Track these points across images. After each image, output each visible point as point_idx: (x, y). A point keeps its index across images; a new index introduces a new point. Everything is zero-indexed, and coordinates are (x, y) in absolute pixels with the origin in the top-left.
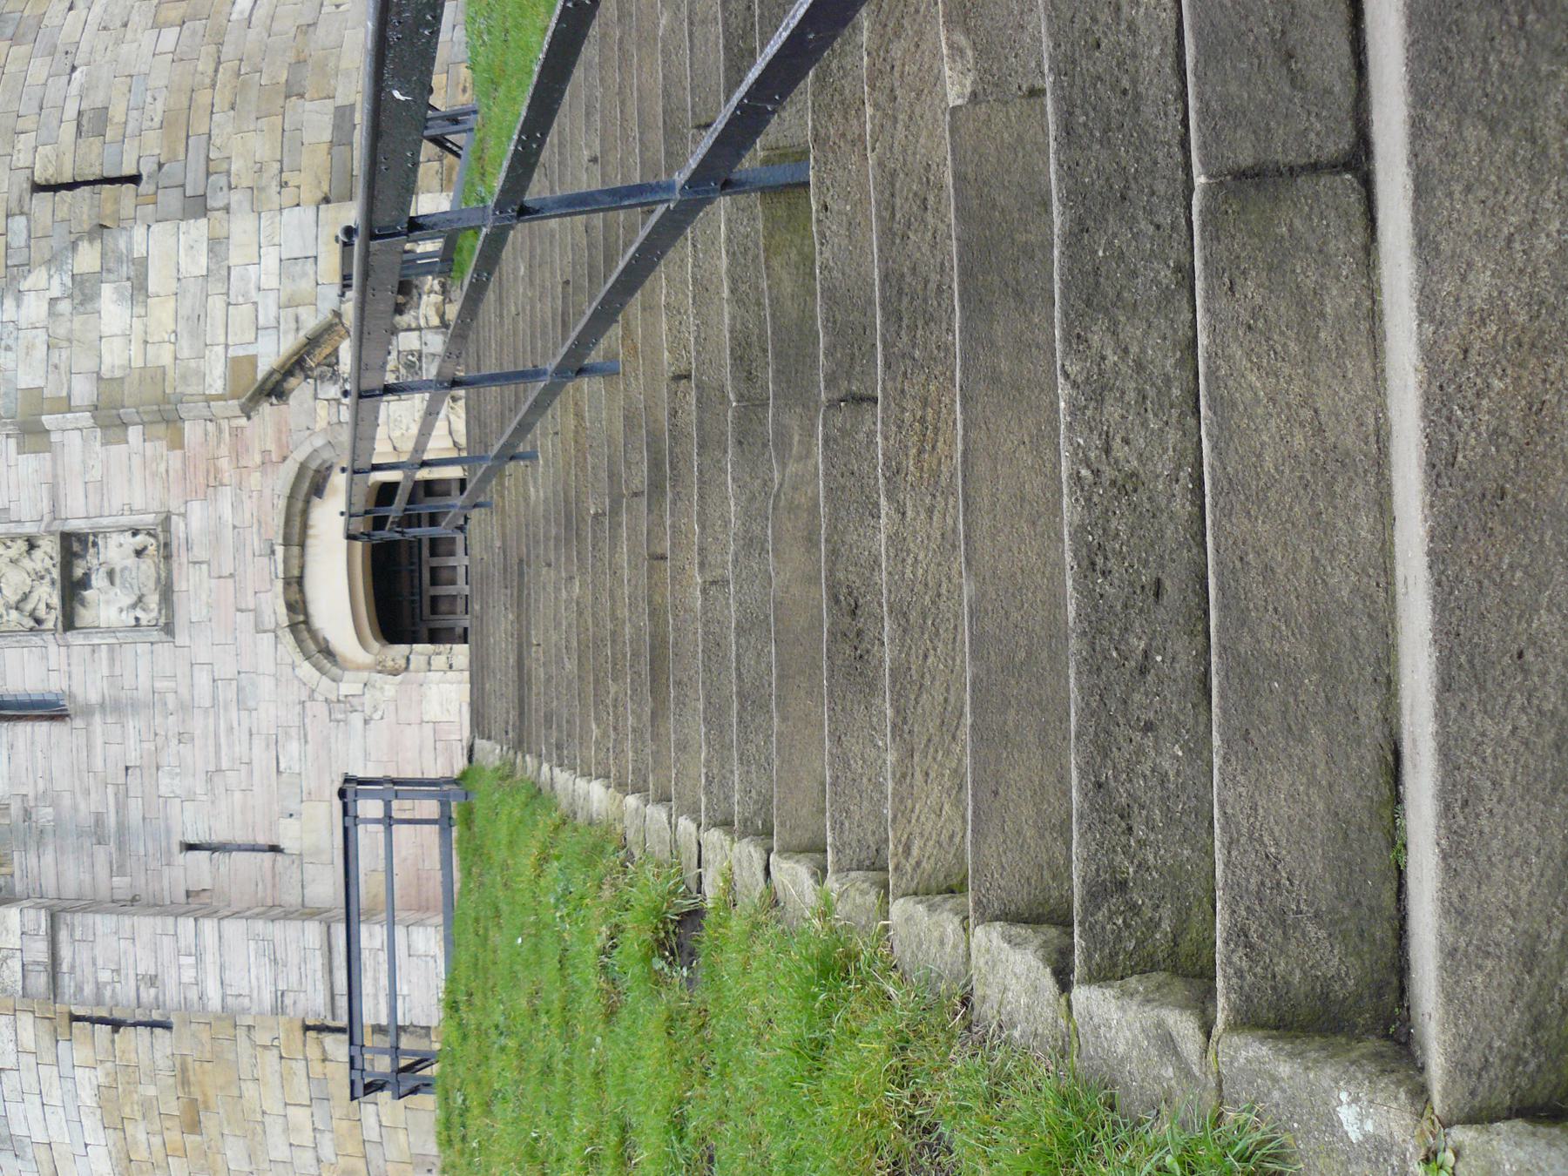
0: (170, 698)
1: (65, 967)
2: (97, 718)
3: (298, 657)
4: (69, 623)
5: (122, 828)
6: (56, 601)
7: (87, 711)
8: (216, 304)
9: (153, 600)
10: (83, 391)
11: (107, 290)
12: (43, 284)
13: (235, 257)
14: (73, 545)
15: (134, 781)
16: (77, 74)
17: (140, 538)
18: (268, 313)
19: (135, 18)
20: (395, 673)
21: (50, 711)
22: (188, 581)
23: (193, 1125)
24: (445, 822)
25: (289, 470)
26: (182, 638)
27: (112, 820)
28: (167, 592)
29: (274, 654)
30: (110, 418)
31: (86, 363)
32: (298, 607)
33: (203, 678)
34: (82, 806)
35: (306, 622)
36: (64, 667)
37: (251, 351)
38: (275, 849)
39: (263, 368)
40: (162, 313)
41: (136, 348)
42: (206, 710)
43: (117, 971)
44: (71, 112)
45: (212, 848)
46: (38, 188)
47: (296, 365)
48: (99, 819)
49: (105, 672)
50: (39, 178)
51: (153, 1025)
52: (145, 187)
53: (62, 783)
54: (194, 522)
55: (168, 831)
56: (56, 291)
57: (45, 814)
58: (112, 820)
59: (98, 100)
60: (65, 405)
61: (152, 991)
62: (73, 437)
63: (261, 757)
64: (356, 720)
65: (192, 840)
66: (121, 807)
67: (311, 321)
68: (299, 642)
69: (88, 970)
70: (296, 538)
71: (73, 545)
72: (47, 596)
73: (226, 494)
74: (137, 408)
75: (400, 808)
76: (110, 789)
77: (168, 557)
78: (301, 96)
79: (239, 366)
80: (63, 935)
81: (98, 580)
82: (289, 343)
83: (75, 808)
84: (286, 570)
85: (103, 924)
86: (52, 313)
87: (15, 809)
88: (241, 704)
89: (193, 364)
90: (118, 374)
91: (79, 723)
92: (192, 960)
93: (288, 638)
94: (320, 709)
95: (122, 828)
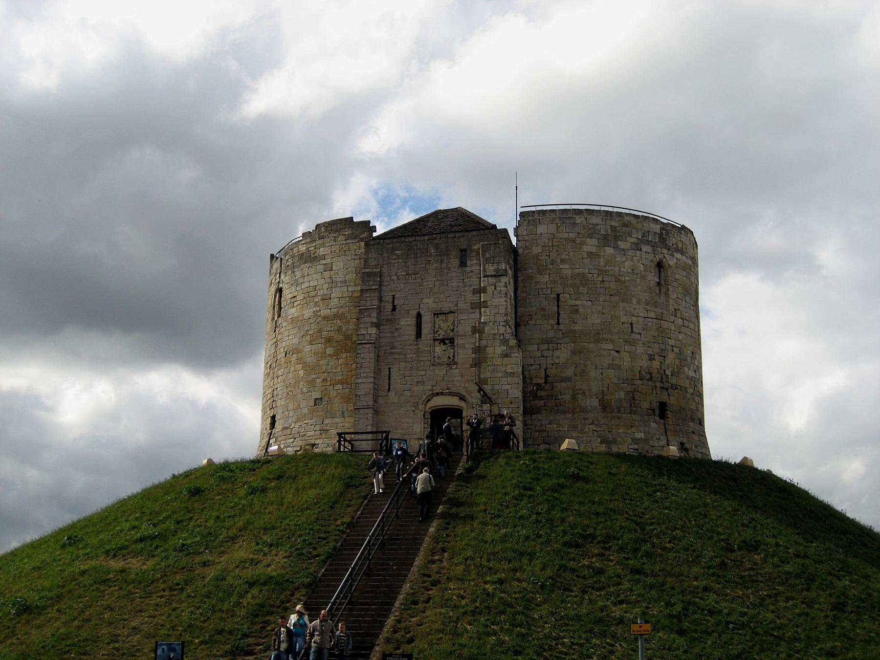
5: (393, 353)
6: (441, 337)
7: (417, 345)
8: (500, 375)
10: (484, 343)
13: (509, 379)
15: (402, 356)
18: (497, 387)
21: (419, 334)
25: (464, 393)
28: (439, 364)
30: (479, 350)
31: (490, 343)
33: (423, 373)
38: (389, 390)
44: (578, 303)
45: (389, 375)
47: (485, 394)
52: (555, 327)
59: (581, 310)
60: (480, 339)
63: (408, 386)
64: (414, 409)
67: (493, 398)
71: (452, 341)
72: (442, 334)
73: (460, 378)
74: (480, 357)
79: (485, 381)
81: (444, 347)
82: (489, 392)
85: (372, 355)
87: (398, 326)
95: (393, 353)
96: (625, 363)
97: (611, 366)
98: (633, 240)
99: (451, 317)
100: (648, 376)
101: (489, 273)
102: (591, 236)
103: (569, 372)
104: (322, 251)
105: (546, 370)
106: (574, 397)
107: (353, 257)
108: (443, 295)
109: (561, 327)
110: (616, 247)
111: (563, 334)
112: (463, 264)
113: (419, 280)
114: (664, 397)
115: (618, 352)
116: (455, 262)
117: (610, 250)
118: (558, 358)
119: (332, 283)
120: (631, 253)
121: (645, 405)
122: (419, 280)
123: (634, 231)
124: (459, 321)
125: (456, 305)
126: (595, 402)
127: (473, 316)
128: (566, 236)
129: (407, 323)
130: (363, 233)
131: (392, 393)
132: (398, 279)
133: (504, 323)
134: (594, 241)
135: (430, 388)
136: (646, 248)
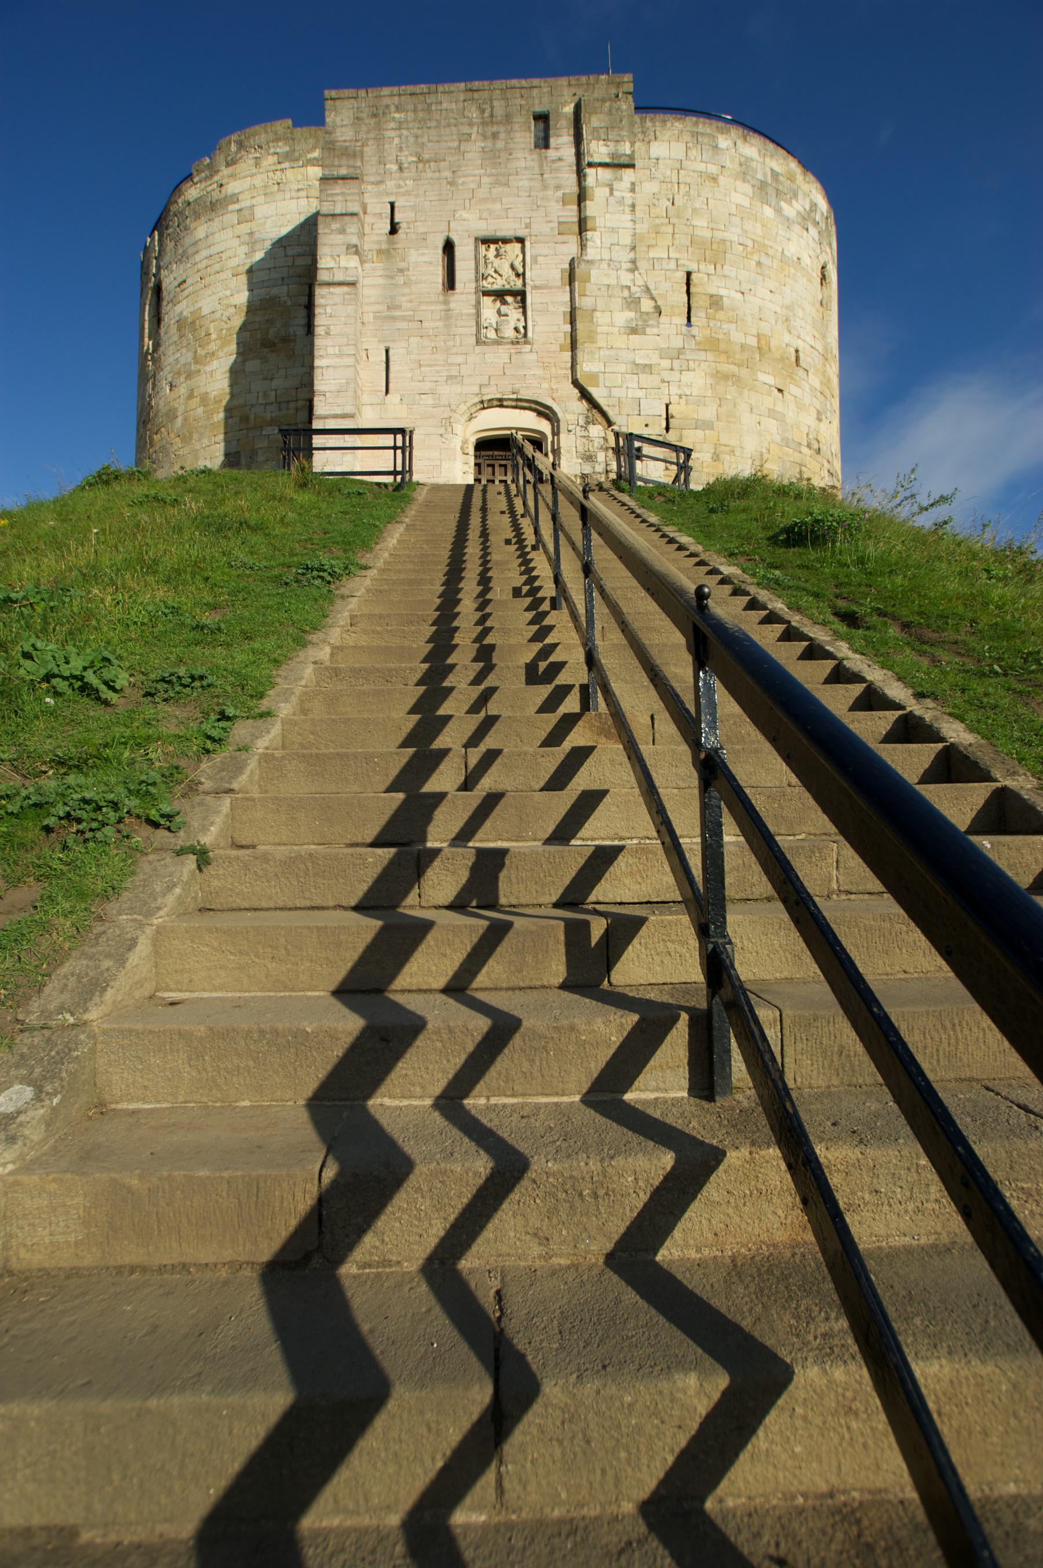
0: (451, 343)
1: (332, 289)
2: (443, 307)
3: (469, 404)
4: (486, 293)
6: (495, 287)
8: (622, 368)
11: (632, 315)
12: (637, 283)
13: (642, 376)
16: (740, 295)
17: (522, 331)
18: (616, 392)
19: (763, 324)
20: (462, 448)
23: (264, 345)
24: (395, 473)
25: (549, 402)
26: (478, 349)
27: (397, 313)
33: (460, 359)
34: (404, 299)
35: (484, 408)
36: (466, 291)
37: (601, 385)
38: (387, 392)
40: (621, 341)
41: (605, 329)
42: (446, 361)
43: (331, 316)
44: (723, 292)
46: (689, 274)
48: (399, 307)
49: (464, 312)
50: (693, 276)
52: (684, 329)
55: (394, 341)
56: (633, 289)
57: (400, 280)
58: (397, 313)
61: (323, 333)
63: (427, 386)
64: (442, 431)
65: (391, 353)
66: (403, 318)
67: (611, 413)
68: (475, 404)
69: (330, 302)
70: (520, 404)
71: (521, 296)
72: (499, 284)
73: (540, 372)
75: (399, 452)
76: (411, 313)
77: (512, 343)
78: (720, 406)
79: (594, 377)
80: (346, 289)
83: (403, 295)
84: (506, 400)
86: (622, 287)
88: (449, 378)
89: (597, 356)
90: (595, 320)
91: (441, 298)
92: (337, 352)
93: (477, 399)
94: (446, 415)
96: (790, 414)
97: (772, 413)
98: (801, 209)
100: (815, 446)
101: (597, 159)
103: (708, 412)
105: (667, 406)
107: (294, 194)
108: (498, 206)
109: (694, 331)
110: (778, 211)
111: (698, 344)
113: (447, 174)
115: (780, 391)
117: (768, 212)
118: (690, 386)
120: (797, 228)
123: (800, 196)
124: (535, 260)
125: (528, 226)
128: (702, 167)
130: (314, 149)
131: (393, 398)
132: (401, 169)
133: (629, 266)
134: (747, 188)
135: (476, 390)
136: (813, 231)
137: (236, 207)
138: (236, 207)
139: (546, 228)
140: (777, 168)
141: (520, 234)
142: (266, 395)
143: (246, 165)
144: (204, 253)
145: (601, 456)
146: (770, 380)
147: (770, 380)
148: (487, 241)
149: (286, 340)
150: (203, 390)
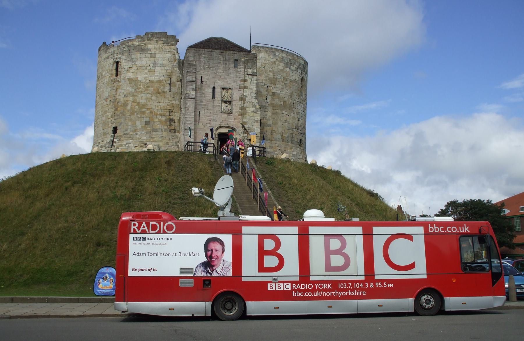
8: (252, 121)
9: (224, 111)
10: (245, 105)
14: (230, 102)
21: (214, 97)
22: (225, 116)
24: (210, 152)
29: (218, 124)
30: (243, 108)
32: (222, 127)
33: (216, 116)
39: (245, 126)
40: (251, 115)
44: (275, 91)
47: (245, 129)
51: (170, 89)
53: (206, 98)
54: (231, 116)
62: (241, 103)
66: (204, 105)
67: (249, 131)
71: (230, 102)
74: (243, 112)
79: (245, 123)
82: (247, 128)
85: (194, 105)
98: (296, 66)
99: (230, 92)
102: (282, 62)
104: (149, 47)
106: (272, 134)
109: (268, 101)
110: (290, 68)
112: (236, 67)
113: (214, 71)
114: (301, 138)
116: (232, 65)
117: (288, 70)
119: (155, 64)
121: (296, 140)
122: (214, 71)
126: (280, 137)
127: (241, 92)
128: (272, 60)
129: (209, 91)
131: (200, 124)
134: (283, 65)
136: (299, 71)
137: (150, 52)
138: (150, 52)
139: (237, 87)
140: (290, 58)
141: (231, 87)
142: (158, 106)
143: (153, 42)
144: (139, 62)
145: (246, 141)
146: (286, 113)
147: (286, 113)
148: (223, 89)
149: (164, 92)
150: (138, 101)
